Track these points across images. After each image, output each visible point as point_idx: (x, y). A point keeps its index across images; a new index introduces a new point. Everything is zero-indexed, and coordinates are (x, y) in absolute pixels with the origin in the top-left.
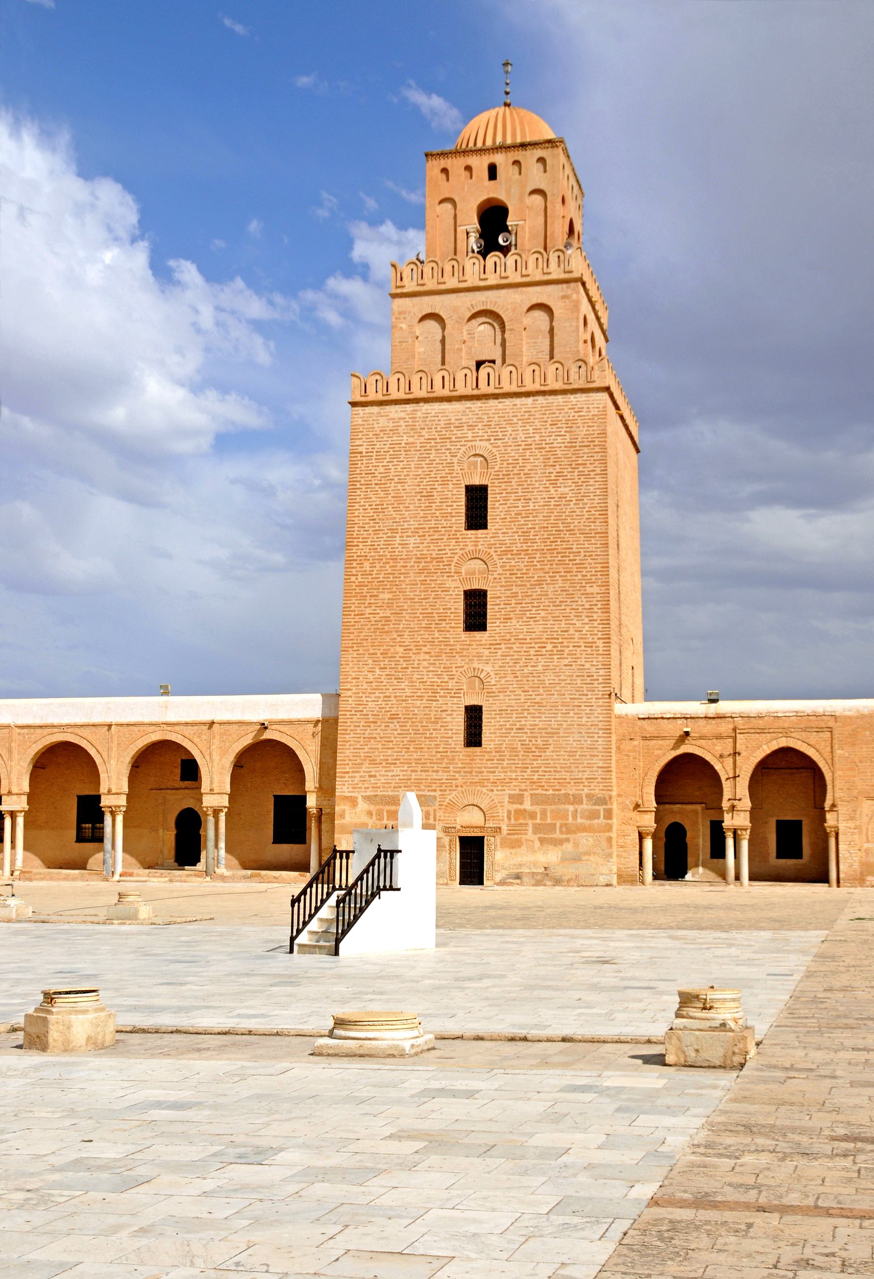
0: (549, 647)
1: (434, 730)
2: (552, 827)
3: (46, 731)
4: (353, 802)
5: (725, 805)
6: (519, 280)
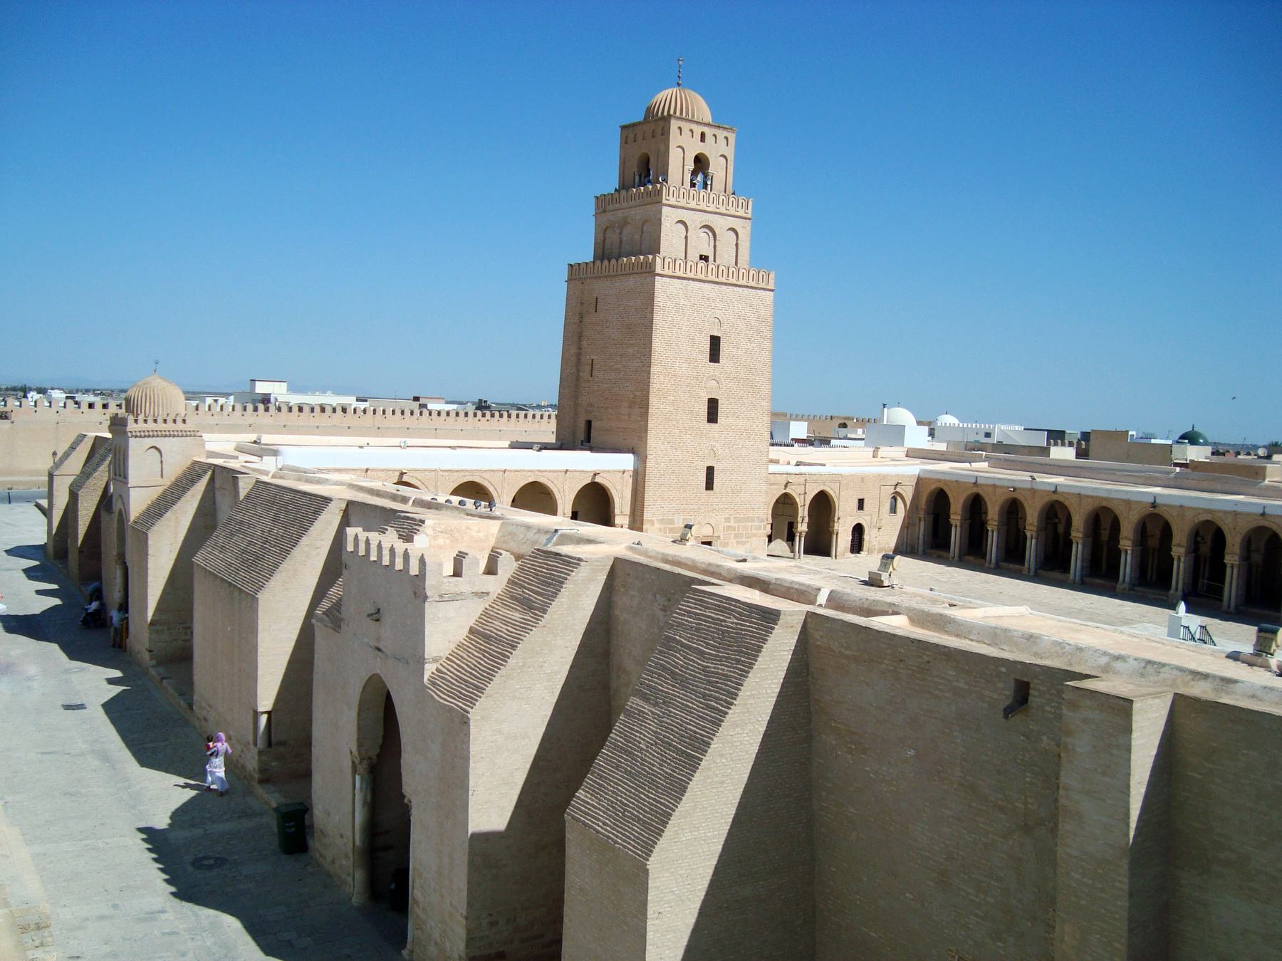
4: (652, 523)
6: (724, 211)
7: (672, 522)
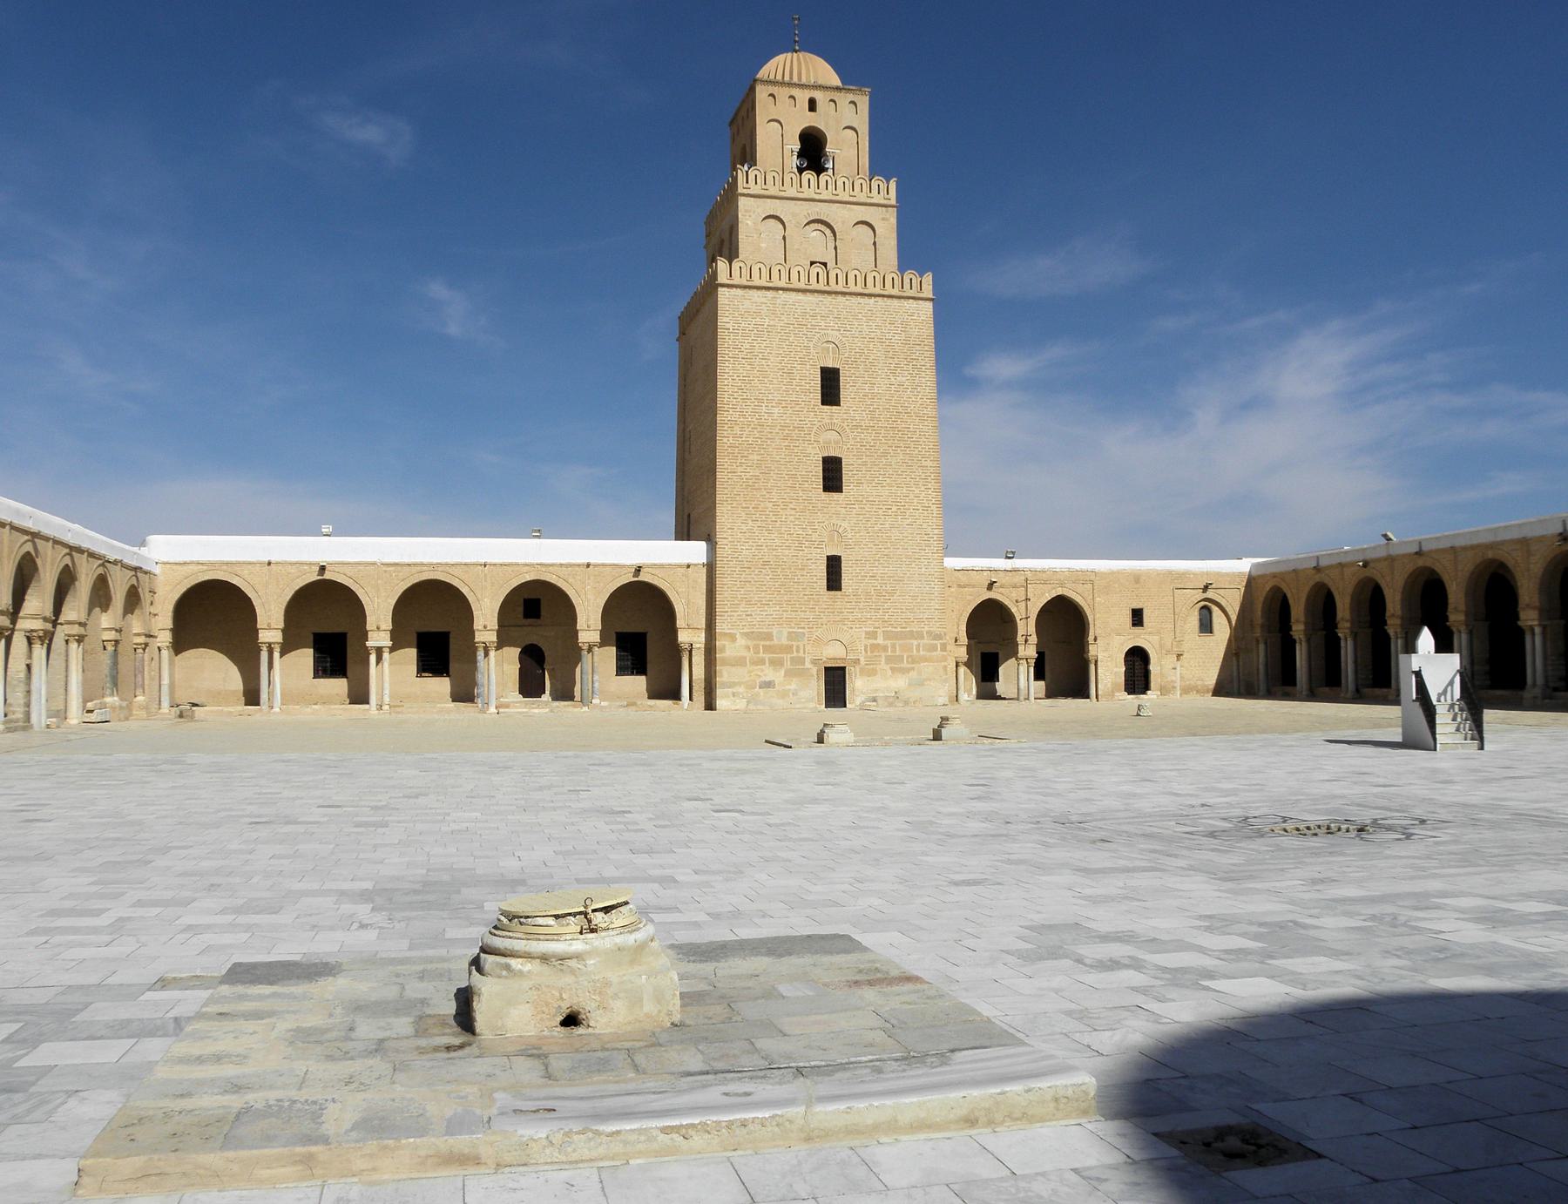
2: (901, 659)
3: (414, 569)
4: (733, 638)
5: (1020, 639)
6: (847, 198)
7: (769, 636)
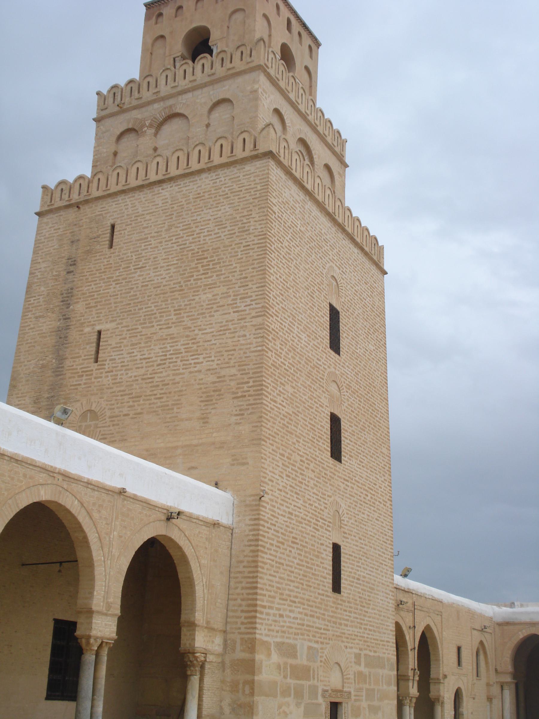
0: (369, 495)
1: (317, 565)
5: (411, 673)
